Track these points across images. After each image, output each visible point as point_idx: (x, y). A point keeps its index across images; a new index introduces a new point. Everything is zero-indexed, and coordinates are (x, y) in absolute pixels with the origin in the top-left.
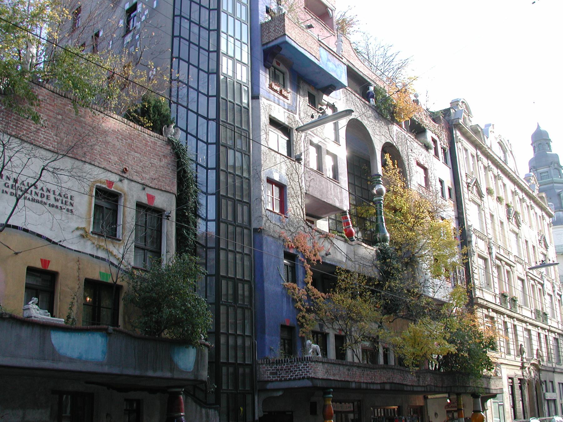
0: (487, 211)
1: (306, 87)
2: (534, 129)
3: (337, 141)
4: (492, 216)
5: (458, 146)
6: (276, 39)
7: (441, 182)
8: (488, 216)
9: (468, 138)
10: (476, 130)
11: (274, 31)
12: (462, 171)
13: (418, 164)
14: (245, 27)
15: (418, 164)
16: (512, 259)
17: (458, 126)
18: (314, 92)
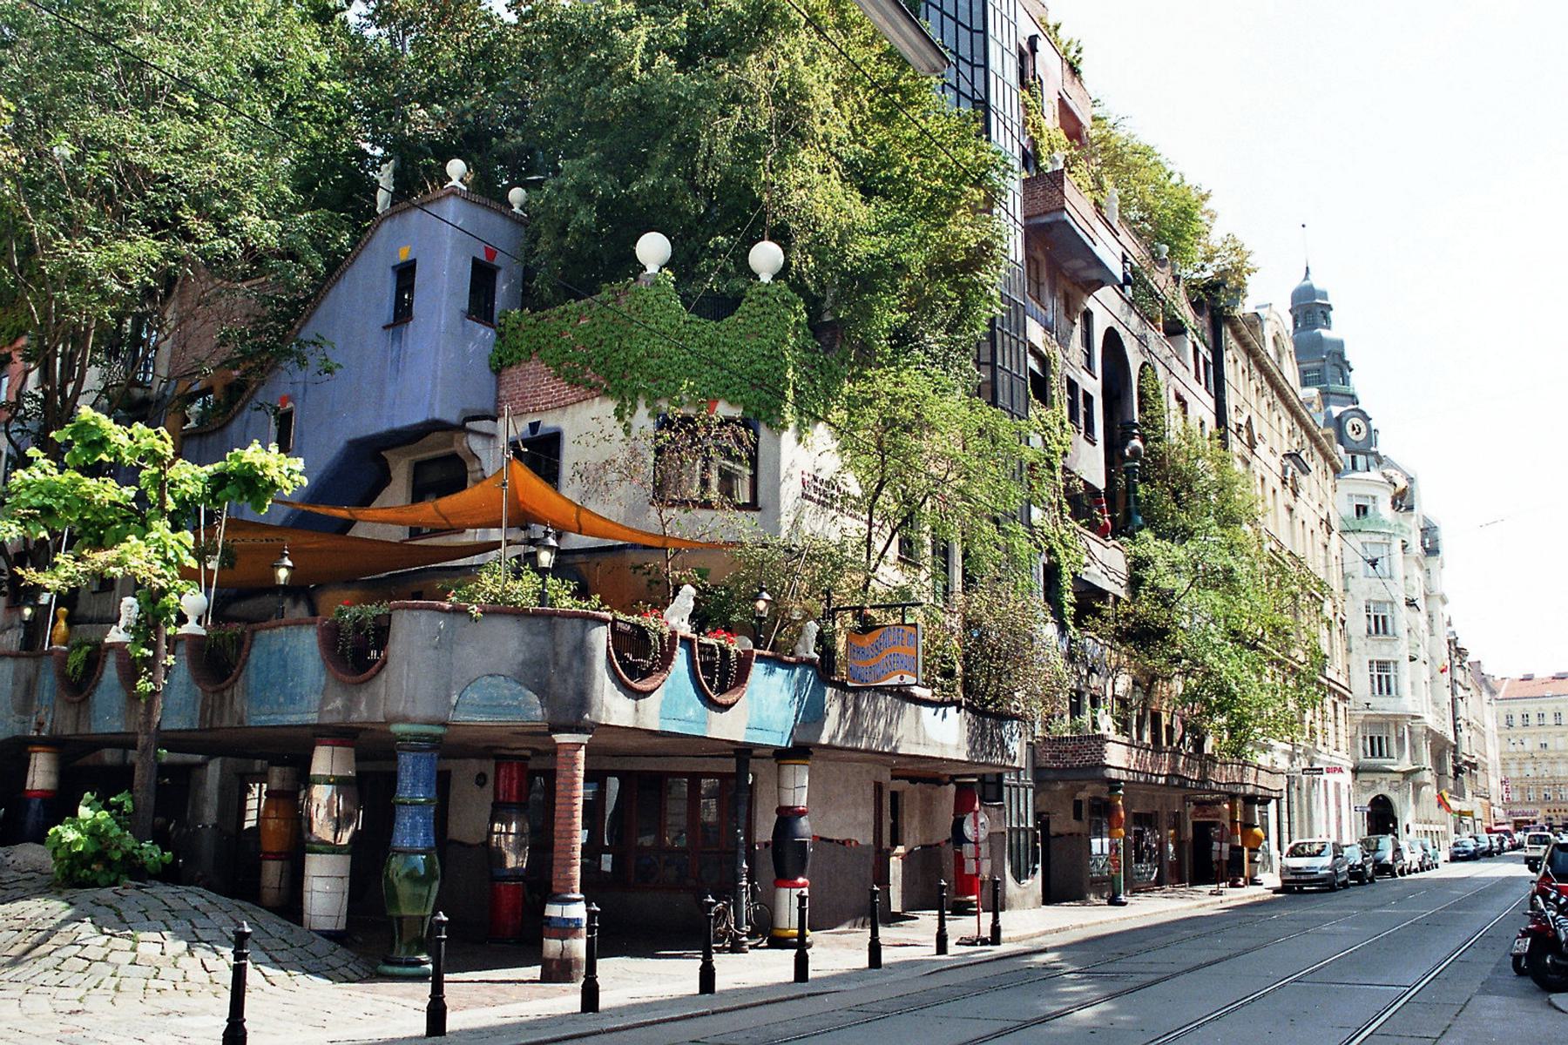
0: (1258, 472)
1: (1063, 284)
2: (1296, 281)
3: (1089, 367)
4: (1263, 479)
5: (1228, 355)
6: (1046, 213)
7: (1202, 424)
8: (1259, 481)
9: (1240, 338)
10: (1255, 321)
11: (1044, 197)
12: (1231, 401)
13: (1179, 398)
14: (1018, 199)
15: (1179, 398)
16: (1284, 554)
17: (1231, 321)
18: (1070, 289)
